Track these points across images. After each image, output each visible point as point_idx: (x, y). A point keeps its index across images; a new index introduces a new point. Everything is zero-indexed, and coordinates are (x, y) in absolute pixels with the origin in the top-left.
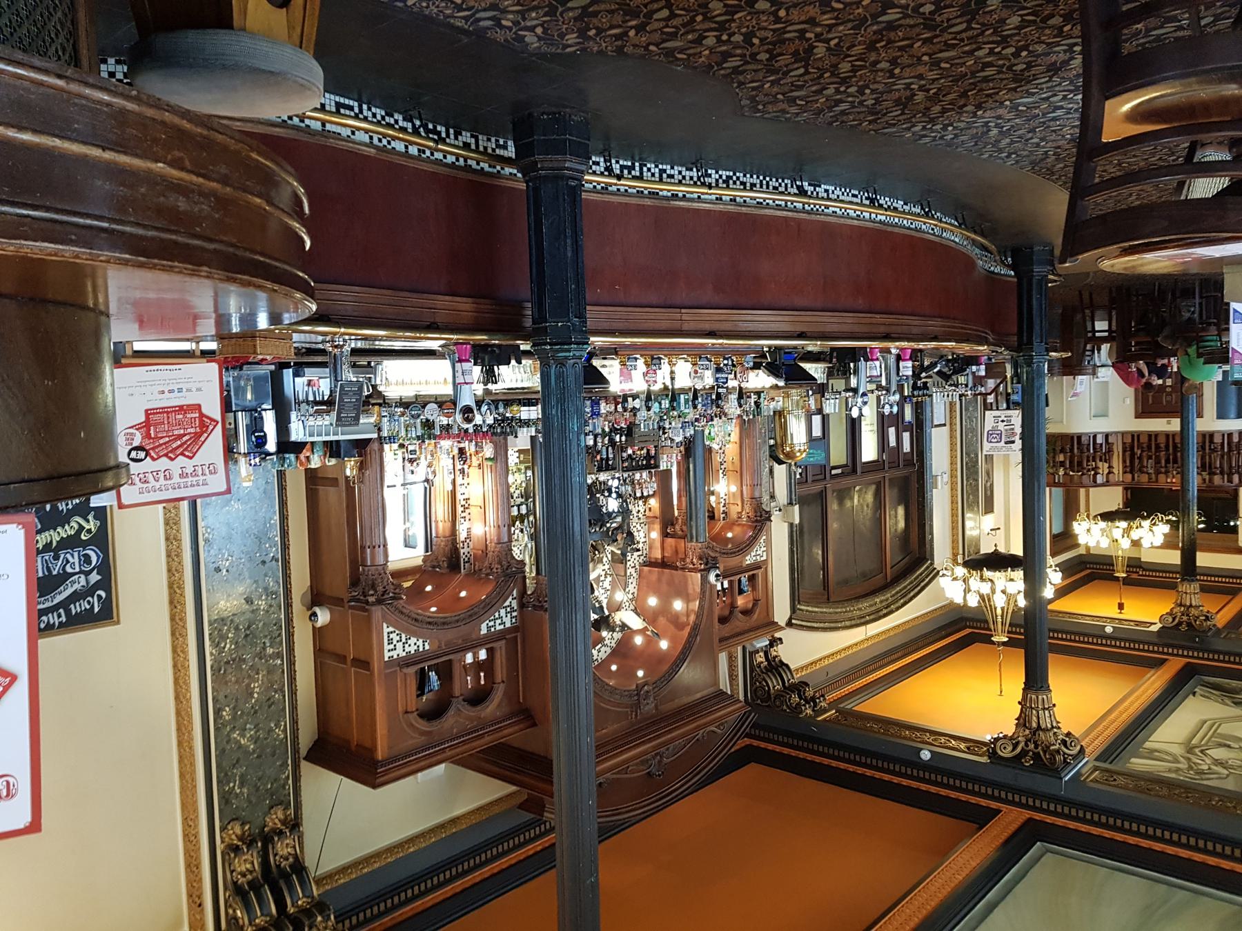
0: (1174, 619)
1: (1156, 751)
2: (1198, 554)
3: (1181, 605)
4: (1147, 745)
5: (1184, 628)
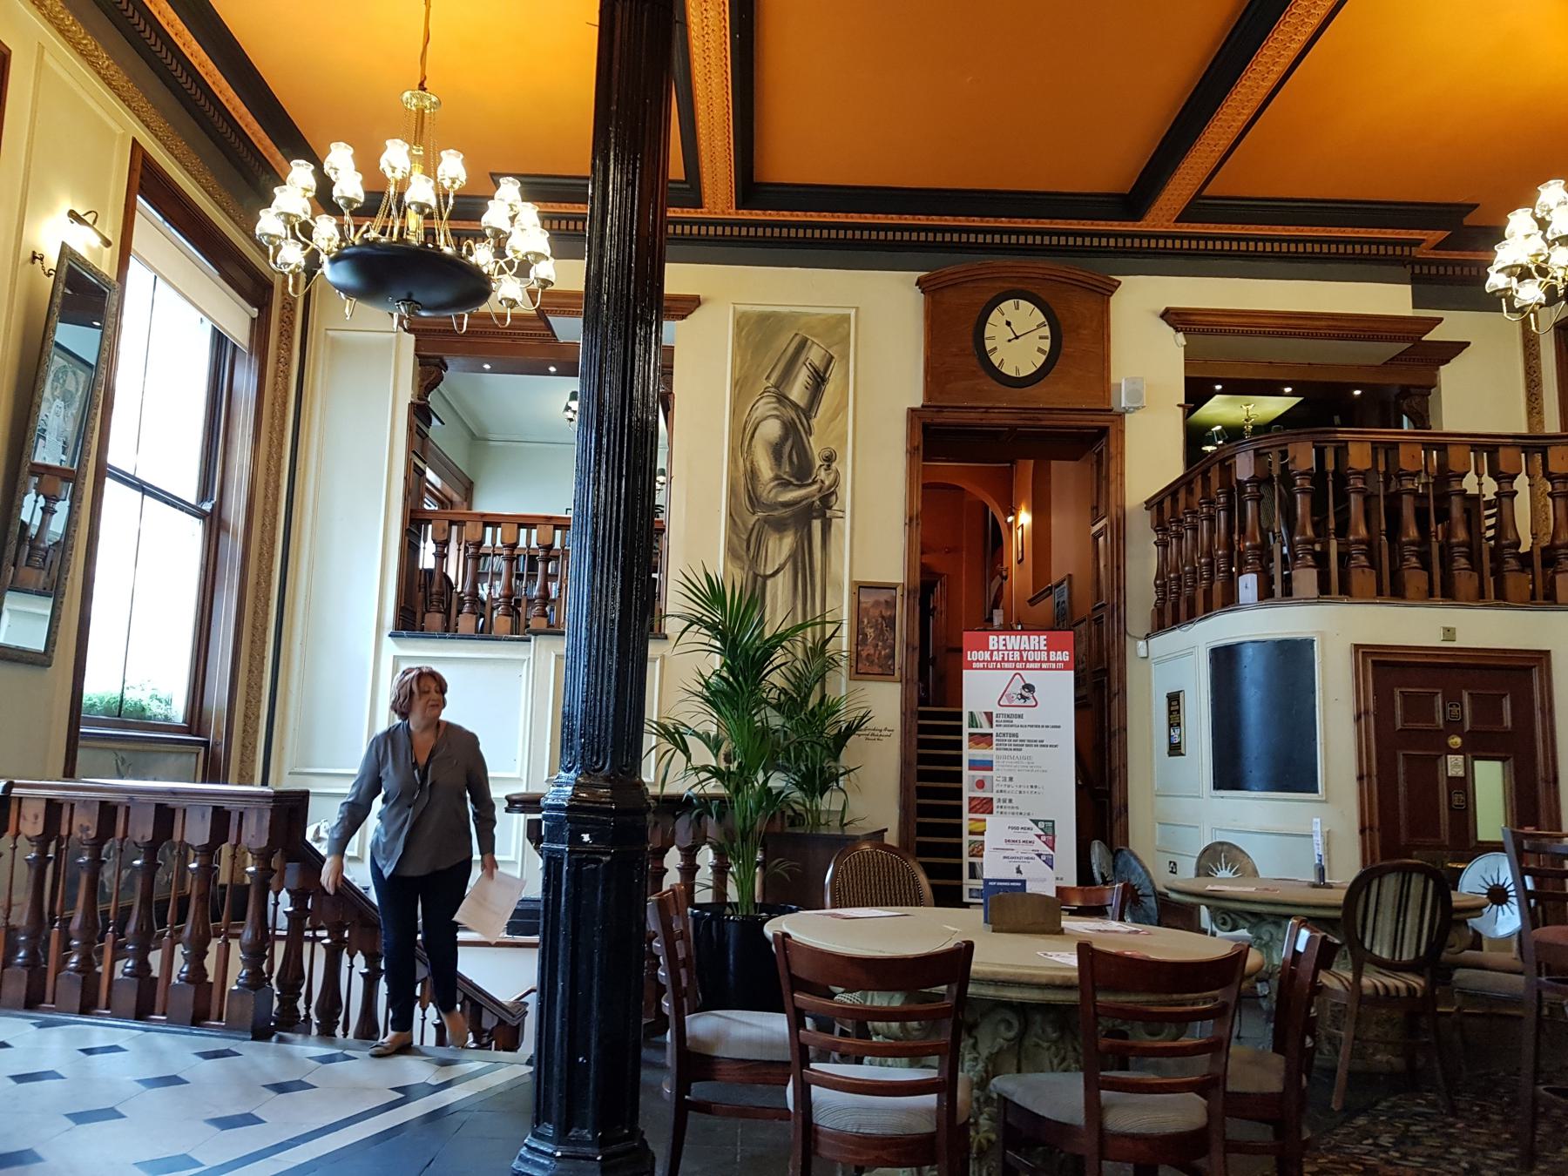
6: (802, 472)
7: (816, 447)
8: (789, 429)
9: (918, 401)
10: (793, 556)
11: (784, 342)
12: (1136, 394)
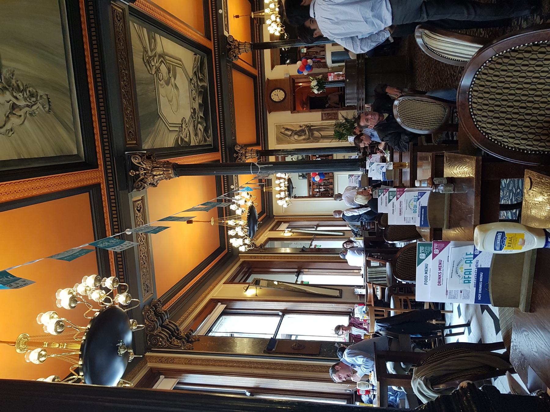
0: (231, 42)
1: (155, 40)
2: (269, 50)
3: (239, 44)
4: (157, 36)
5: (228, 47)
6: (303, 131)
7: (299, 129)
8: (296, 134)
9: (290, 112)
10: (317, 131)
11: (281, 136)
12: (287, 74)
